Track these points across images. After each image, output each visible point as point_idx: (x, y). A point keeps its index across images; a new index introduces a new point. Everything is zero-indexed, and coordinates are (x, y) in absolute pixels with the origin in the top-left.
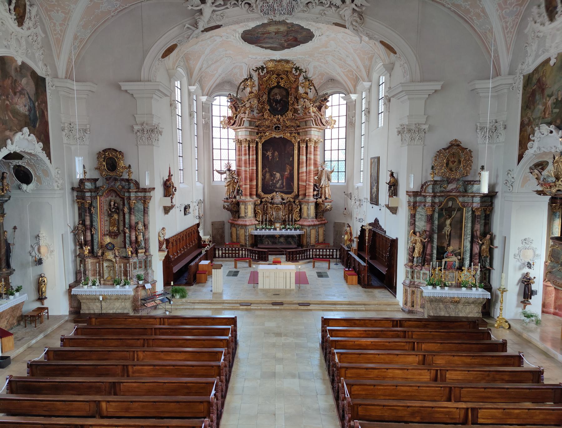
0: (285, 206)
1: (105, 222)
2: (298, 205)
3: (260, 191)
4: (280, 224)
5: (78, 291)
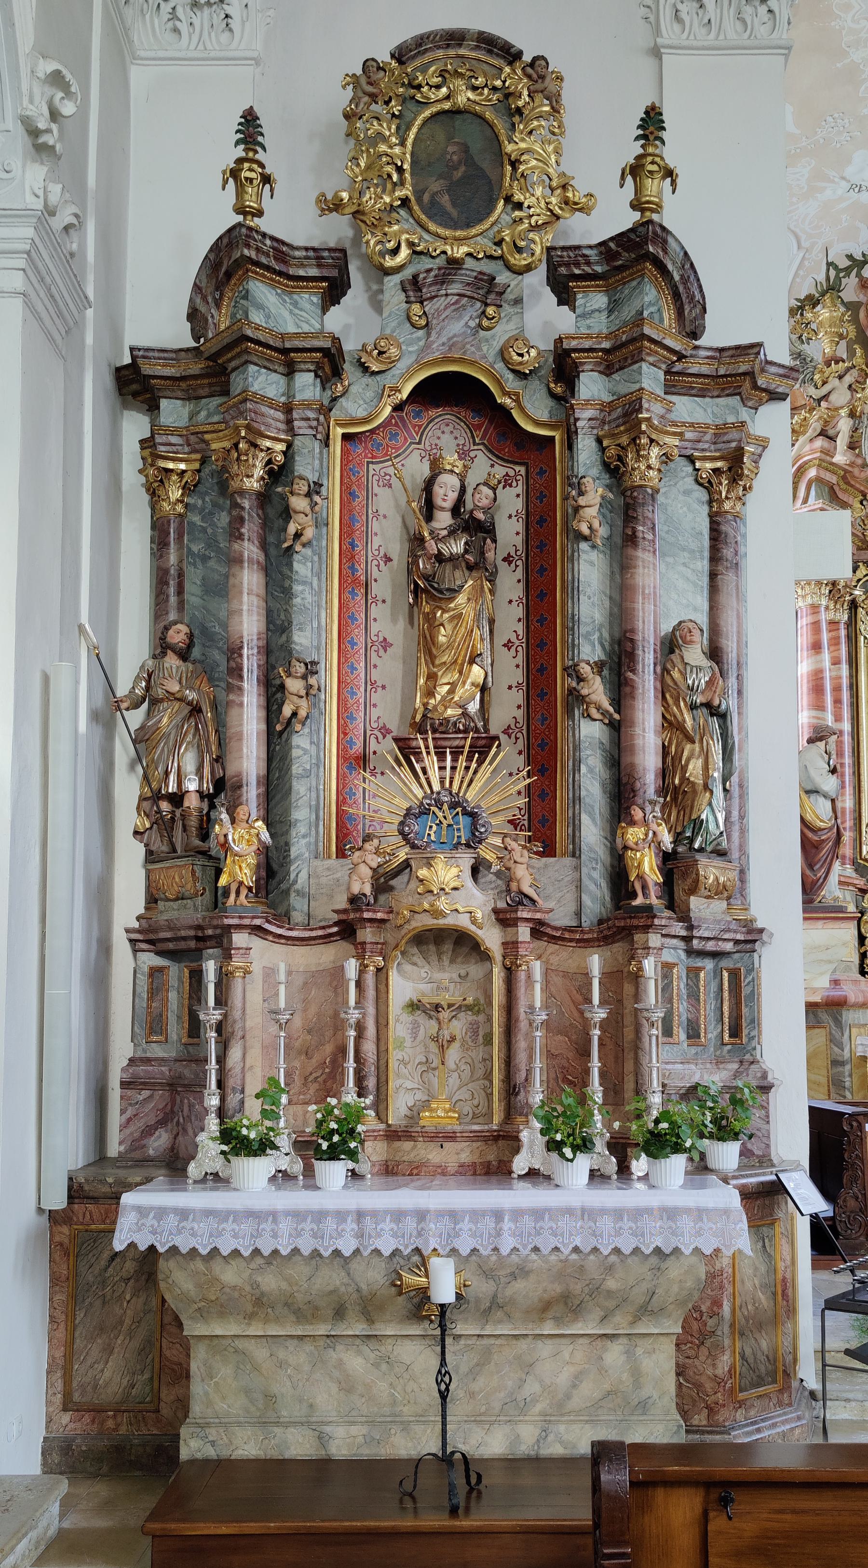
1: (374, 659)
5: (184, 1214)
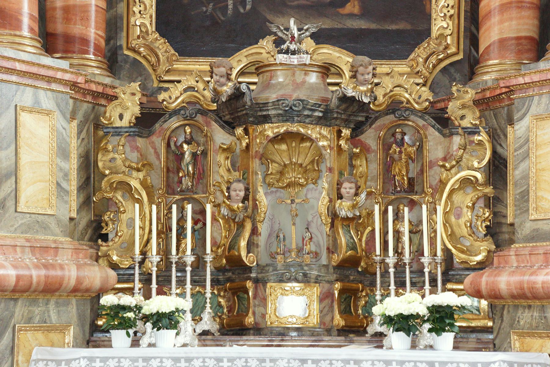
0: (353, 138)
2: (473, 131)
3: (144, 34)
4: (316, 291)
